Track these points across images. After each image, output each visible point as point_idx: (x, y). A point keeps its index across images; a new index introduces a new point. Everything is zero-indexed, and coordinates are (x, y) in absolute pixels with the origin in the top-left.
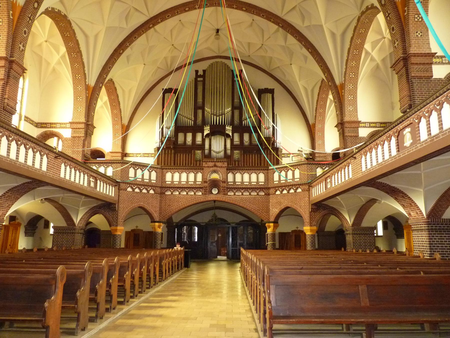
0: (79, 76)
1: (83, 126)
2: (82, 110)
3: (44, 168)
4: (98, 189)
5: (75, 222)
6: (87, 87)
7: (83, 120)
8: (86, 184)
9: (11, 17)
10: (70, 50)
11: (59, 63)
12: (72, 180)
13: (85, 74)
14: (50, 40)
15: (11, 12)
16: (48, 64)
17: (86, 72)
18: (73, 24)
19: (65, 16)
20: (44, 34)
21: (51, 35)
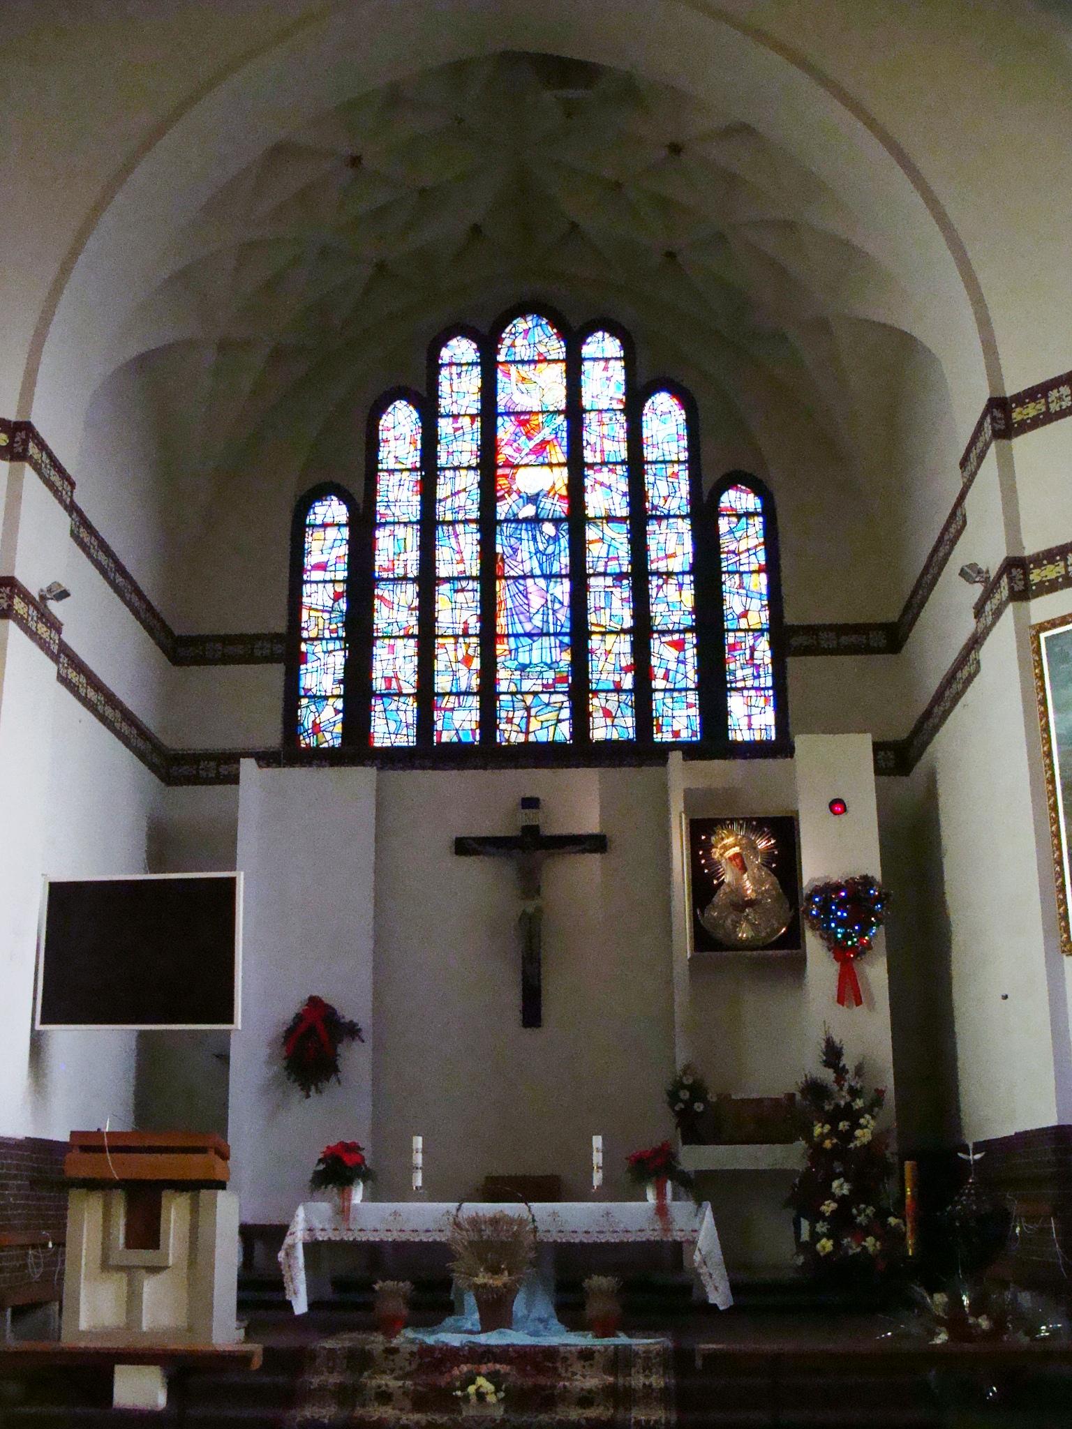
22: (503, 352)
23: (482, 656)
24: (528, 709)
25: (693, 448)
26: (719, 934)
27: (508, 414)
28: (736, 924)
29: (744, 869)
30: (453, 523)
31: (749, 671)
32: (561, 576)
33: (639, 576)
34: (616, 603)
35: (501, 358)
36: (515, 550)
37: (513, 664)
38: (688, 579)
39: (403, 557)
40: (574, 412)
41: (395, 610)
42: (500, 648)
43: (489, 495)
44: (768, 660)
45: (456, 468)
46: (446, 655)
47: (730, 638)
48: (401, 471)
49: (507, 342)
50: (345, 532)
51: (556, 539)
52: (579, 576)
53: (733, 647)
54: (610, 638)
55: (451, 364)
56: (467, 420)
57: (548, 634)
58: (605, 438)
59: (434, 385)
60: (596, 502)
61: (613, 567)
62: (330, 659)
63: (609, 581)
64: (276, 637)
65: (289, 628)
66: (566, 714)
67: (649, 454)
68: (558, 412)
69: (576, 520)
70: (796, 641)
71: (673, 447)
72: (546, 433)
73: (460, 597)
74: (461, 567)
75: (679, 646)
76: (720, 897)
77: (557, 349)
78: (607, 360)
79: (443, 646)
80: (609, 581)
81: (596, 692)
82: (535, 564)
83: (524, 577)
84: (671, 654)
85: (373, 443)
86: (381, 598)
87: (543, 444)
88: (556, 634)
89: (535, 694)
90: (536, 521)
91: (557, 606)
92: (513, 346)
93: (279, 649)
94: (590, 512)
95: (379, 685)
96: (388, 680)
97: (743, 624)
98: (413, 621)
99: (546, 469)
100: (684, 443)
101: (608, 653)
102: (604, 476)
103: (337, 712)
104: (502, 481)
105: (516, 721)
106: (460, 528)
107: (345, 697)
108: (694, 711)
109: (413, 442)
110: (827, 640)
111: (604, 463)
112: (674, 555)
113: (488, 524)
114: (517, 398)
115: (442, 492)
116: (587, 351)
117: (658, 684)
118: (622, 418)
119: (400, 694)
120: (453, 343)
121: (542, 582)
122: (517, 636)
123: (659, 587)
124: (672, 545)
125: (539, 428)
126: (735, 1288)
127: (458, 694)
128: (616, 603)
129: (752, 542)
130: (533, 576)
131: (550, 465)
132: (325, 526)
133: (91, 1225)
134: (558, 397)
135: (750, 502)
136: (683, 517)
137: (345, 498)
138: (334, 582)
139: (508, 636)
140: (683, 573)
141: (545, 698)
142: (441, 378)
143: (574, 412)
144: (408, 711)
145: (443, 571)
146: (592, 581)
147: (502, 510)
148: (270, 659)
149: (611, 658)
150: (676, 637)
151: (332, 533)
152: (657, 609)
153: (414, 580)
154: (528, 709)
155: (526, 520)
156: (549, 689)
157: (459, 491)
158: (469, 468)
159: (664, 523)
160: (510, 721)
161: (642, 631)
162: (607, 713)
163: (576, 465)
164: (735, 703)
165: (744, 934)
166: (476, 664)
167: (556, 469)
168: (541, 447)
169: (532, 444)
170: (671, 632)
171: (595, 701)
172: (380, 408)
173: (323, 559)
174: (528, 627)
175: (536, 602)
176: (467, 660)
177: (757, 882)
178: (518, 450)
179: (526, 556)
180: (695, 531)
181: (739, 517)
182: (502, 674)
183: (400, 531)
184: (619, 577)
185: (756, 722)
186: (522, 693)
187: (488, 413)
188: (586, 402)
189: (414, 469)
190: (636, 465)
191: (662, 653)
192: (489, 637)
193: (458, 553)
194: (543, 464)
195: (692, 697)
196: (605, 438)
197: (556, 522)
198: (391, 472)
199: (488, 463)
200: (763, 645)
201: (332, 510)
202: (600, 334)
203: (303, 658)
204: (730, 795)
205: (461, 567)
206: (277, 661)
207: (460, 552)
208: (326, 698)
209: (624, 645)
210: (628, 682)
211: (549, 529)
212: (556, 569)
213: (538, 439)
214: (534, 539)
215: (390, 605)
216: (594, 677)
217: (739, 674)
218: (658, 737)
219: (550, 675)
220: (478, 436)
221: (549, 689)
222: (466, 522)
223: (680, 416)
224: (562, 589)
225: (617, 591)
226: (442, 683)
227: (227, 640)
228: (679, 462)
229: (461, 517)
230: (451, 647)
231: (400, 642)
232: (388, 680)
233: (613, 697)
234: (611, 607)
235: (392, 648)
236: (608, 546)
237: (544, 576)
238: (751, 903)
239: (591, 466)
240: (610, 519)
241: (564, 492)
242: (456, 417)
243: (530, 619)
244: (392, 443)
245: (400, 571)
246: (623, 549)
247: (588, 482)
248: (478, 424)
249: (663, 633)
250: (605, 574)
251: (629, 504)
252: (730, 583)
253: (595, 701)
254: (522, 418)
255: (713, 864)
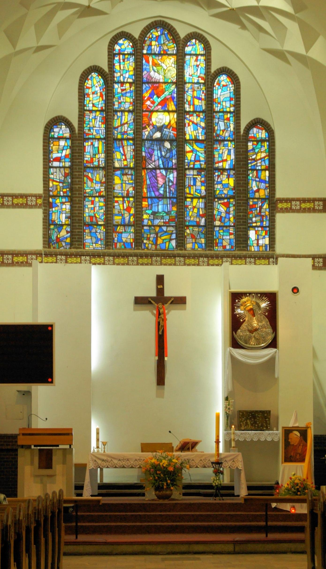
22: (146, 48)
23: (136, 208)
24: (157, 234)
25: (237, 105)
27: (148, 83)
30: (122, 140)
31: (258, 218)
32: (173, 169)
33: (210, 170)
34: (198, 184)
35: (145, 52)
36: (151, 155)
37: (150, 212)
38: (232, 172)
39: (97, 156)
40: (180, 82)
41: (94, 183)
42: (145, 203)
43: (139, 125)
44: (267, 213)
45: (123, 111)
46: (119, 206)
48: (96, 111)
49: (148, 43)
50: (69, 142)
51: (170, 150)
52: (181, 168)
54: (195, 201)
55: (119, 54)
56: (128, 85)
57: (167, 198)
58: (194, 98)
59: (111, 65)
60: (190, 132)
61: (197, 165)
62: (64, 207)
63: (195, 172)
64: (37, 196)
65: (44, 190)
66: (174, 236)
67: (217, 108)
68: (173, 83)
69: (180, 141)
70: (280, 206)
71: (228, 105)
72: (167, 94)
73: (125, 178)
74: (125, 163)
75: (227, 205)
77: (172, 47)
78: (197, 55)
79: (117, 202)
80: (195, 172)
81: (188, 227)
82: (161, 162)
83: (155, 169)
84: (223, 209)
85: (82, 95)
86: (88, 177)
87: (165, 99)
88: (170, 198)
89: (160, 226)
90: (161, 140)
91: (171, 184)
92: (150, 45)
93: (40, 201)
94: (187, 137)
95: (87, 220)
96: (91, 217)
97: (257, 195)
98: (103, 189)
99: (166, 114)
100: (233, 102)
101: (194, 207)
102: (194, 119)
103: (67, 232)
104: (145, 119)
105: (151, 239)
106: (125, 143)
107: (71, 225)
108: (232, 237)
109: (101, 95)
110: (296, 205)
111: (194, 112)
112: (226, 160)
113: (138, 141)
114: (152, 73)
115: (117, 123)
116: (188, 49)
117: (217, 223)
118: (203, 88)
119: (98, 225)
120: (121, 42)
121: (164, 172)
122: (151, 198)
123: (219, 176)
124: (226, 156)
125: (163, 92)
126: (249, 488)
127: (124, 225)
128: (198, 184)
129: (263, 155)
130: (160, 169)
131: (169, 112)
132: (59, 138)
134: (172, 74)
135: (262, 134)
136: (231, 141)
137: (69, 124)
138: (64, 167)
139: (148, 198)
140: (230, 169)
141: (164, 229)
142: (115, 62)
143: (180, 82)
144: (101, 232)
145: (117, 165)
146: (187, 172)
147: (146, 133)
148: (36, 206)
149: (196, 210)
150: (226, 201)
151: (62, 143)
152: (218, 187)
153: (103, 168)
154: (157, 234)
155: (157, 140)
156: (167, 224)
157: (125, 122)
158: (129, 111)
159: (222, 144)
160: (148, 239)
161: (210, 198)
162: (193, 237)
163: (181, 113)
164: (252, 234)
166: (132, 211)
167: (171, 114)
168: (164, 103)
169: (159, 100)
170: (223, 198)
171: (188, 231)
172: (85, 76)
173: (59, 155)
174: (157, 194)
175: (161, 181)
176: (128, 209)
177: (259, 321)
178: (153, 103)
179: (156, 158)
180: (236, 148)
181: (258, 141)
182: (145, 216)
183: (96, 144)
184: (200, 170)
185: (261, 242)
186: (154, 226)
187: (139, 80)
188: (187, 78)
189: (101, 111)
190: (209, 113)
191: (220, 209)
192: (139, 197)
193: (124, 156)
194: (165, 111)
195: (232, 230)
196: (194, 98)
197: (171, 141)
198: (91, 111)
199: (139, 111)
200: (266, 206)
201: (62, 131)
202: (194, 41)
203: (51, 205)
205: (125, 163)
206: (39, 207)
207: (125, 155)
208: (62, 225)
209: (201, 203)
210: (203, 222)
211: (167, 145)
212: (170, 165)
213: (163, 97)
214: (160, 150)
215: (91, 180)
216: (188, 218)
217: (254, 219)
219: (167, 218)
220: (133, 94)
221: (167, 224)
222: (128, 139)
223: (231, 87)
224: (172, 176)
225: (199, 178)
226: (117, 219)
227: (15, 196)
228: (230, 112)
229: (125, 136)
230: (120, 203)
231: (97, 199)
232: (91, 217)
233: (196, 229)
234: (197, 187)
235: (93, 202)
236: (194, 154)
237: (164, 168)
239: (188, 113)
240: (196, 140)
241: (175, 126)
242: (122, 83)
243: (158, 190)
244: (91, 96)
245: (96, 164)
246: (202, 157)
247: (187, 122)
248: (133, 88)
249: (220, 199)
250: (193, 169)
251: (205, 134)
252: (252, 175)
253: (188, 231)
254: (156, 86)
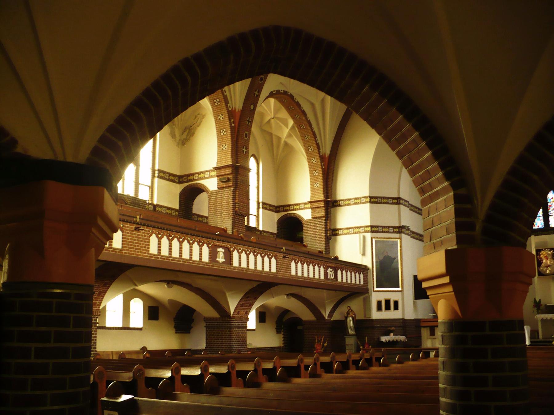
0: (311, 149)
1: (322, 204)
2: (319, 185)
3: (274, 270)
4: (339, 280)
5: (324, 315)
6: (322, 158)
7: (322, 197)
8: (322, 277)
9: (233, 125)
10: (298, 124)
11: (289, 135)
12: (306, 275)
13: (318, 145)
14: (276, 116)
15: (232, 120)
16: (279, 139)
17: (319, 141)
18: (295, 96)
19: (285, 93)
20: (271, 112)
21: (276, 111)
26: (543, 272)
28: (547, 270)
29: (547, 259)
47: (549, 204)
53: (550, 206)
76: (543, 265)
108: (542, 221)
133: (425, 333)
165: (548, 272)
177: (551, 262)
204: (545, 243)
218: (534, 228)
238: (549, 266)
255: (541, 258)
